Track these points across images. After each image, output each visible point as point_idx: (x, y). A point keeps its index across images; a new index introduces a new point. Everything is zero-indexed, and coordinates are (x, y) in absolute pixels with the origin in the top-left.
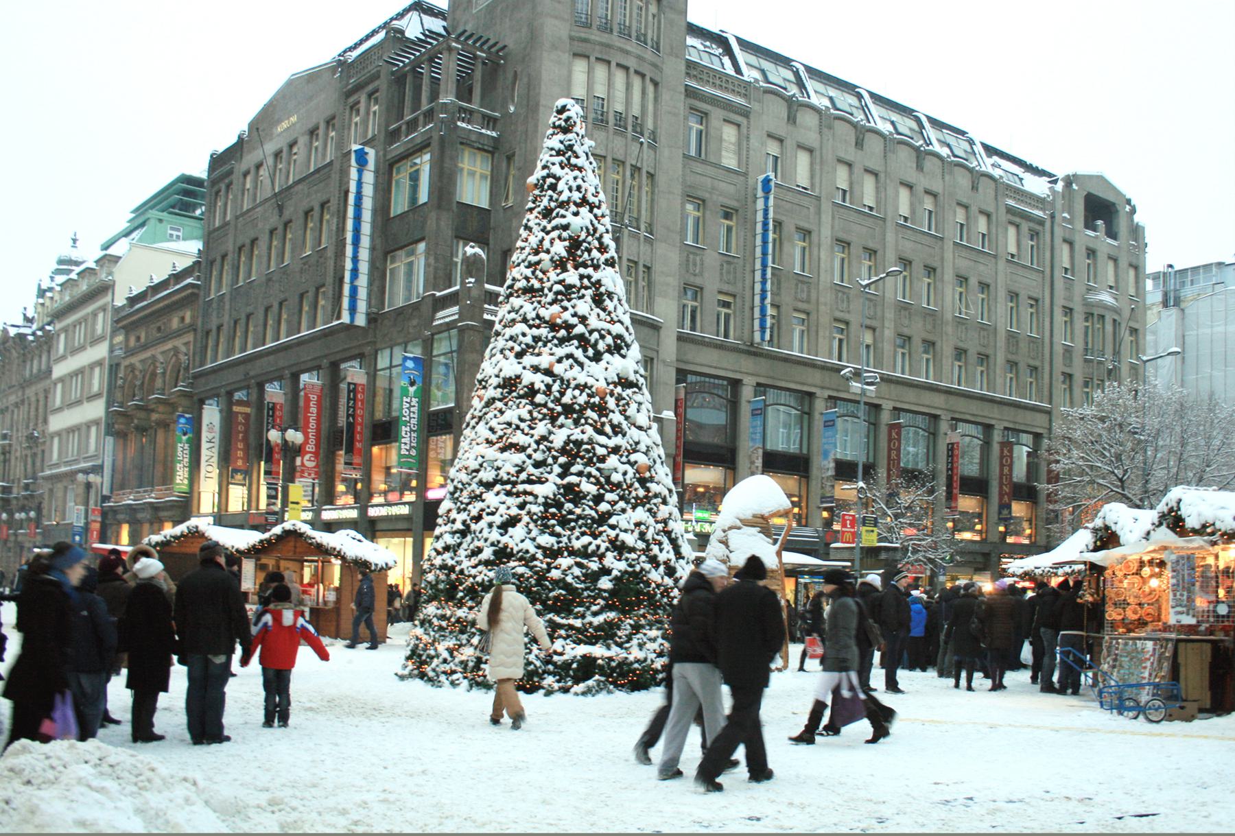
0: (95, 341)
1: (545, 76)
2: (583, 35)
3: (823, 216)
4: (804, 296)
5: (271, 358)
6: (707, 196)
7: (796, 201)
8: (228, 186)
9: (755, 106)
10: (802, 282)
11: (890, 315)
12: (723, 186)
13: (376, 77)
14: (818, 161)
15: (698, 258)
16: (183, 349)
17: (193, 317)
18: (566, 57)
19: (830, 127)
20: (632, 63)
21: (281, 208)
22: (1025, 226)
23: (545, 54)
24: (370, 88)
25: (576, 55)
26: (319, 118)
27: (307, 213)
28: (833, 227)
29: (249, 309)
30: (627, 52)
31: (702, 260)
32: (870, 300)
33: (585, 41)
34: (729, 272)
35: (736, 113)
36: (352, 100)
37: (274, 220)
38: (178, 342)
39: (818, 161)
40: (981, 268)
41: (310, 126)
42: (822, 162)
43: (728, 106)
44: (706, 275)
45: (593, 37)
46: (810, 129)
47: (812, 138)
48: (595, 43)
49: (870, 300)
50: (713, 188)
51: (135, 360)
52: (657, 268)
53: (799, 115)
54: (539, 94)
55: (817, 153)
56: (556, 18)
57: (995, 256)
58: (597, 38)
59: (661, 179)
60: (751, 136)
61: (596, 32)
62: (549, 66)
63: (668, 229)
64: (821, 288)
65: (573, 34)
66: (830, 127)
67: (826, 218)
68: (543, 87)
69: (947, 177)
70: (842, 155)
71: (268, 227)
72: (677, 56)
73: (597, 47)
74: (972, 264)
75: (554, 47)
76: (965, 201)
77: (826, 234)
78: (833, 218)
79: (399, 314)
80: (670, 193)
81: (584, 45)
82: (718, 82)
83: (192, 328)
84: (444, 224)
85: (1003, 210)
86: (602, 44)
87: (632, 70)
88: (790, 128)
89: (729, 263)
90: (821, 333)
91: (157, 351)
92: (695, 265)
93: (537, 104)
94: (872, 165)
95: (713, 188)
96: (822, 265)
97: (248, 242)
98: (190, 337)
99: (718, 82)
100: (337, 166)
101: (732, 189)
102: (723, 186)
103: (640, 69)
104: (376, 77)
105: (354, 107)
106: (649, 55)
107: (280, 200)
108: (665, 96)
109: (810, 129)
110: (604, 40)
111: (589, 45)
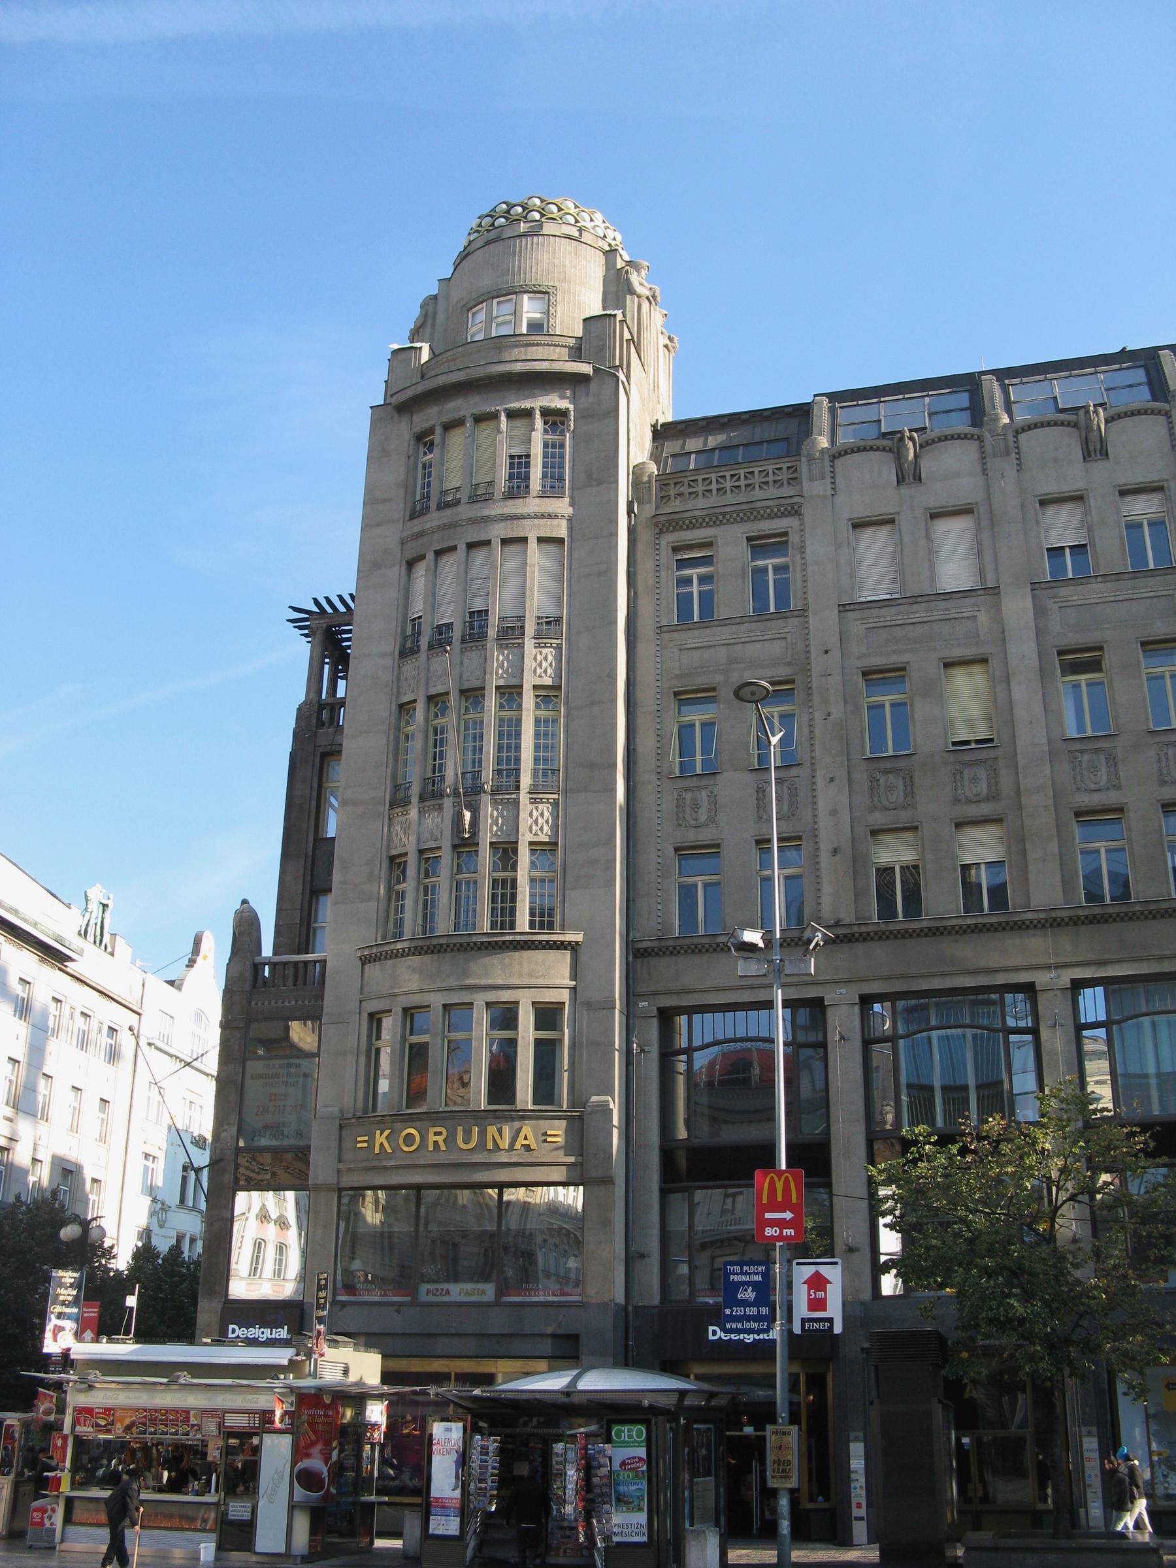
12: (753, 650)
14: (985, 522)
15: (704, 794)
35: (770, 517)
45: (429, 525)
47: (967, 489)
50: (732, 660)
60: (808, 543)
64: (1021, 761)
70: (1051, 487)
77: (1023, 651)
80: (593, 703)
90: (1033, 853)
94: (1137, 477)
96: (1020, 713)
101: (776, 648)
102: (753, 650)
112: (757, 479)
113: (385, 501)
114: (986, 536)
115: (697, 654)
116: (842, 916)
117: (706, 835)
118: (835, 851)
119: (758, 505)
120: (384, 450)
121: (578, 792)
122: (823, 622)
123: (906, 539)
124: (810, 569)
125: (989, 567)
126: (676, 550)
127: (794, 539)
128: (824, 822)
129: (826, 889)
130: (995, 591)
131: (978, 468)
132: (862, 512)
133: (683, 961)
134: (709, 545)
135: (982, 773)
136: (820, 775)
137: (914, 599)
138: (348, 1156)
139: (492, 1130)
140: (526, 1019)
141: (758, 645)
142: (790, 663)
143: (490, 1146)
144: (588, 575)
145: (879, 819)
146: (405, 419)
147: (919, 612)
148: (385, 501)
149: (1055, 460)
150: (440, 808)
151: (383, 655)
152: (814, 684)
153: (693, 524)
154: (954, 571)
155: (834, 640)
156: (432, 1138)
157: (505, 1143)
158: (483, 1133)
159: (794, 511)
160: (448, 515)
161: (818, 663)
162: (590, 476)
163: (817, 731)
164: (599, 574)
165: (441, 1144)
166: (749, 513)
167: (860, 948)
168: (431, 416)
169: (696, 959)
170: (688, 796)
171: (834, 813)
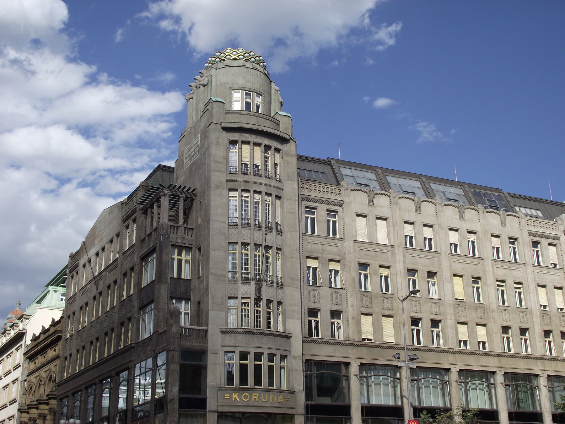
0: (15, 368)
1: (212, 204)
2: (234, 178)
3: (397, 257)
4: (389, 306)
5: (91, 372)
6: (319, 255)
7: (379, 250)
8: (77, 273)
9: (346, 200)
10: (387, 298)
11: (450, 311)
13: (134, 211)
14: (391, 224)
15: (316, 292)
16: (54, 369)
17: (59, 349)
18: (225, 192)
19: (397, 204)
20: (263, 189)
21: (97, 284)
22: (544, 242)
23: (212, 192)
24: (133, 217)
25: (230, 190)
26: (113, 234)
27: (109, 287)
28: (404, 262)
29: (83, 344)
30: (260, 184)
31: (319, 293)
32: (436, 303)
33: (236, 181)
34: (337, 298)
35: (334, 205)
36: (126, 223)
37: (94, 292)
38: (51, 366)
39: (391, 224)
40: (515, 273)
41: (110, 238)
42: (394, 225)
43: (328, 202)
44: (321, 301)
45: (239, 179)
46: (384, 207)
48: (240, 181)
49: (436, 303)
50: (323, 250)
51: (32, 378)
52: (286, 302)
53: (376, 201)
54: (210, 214)
55: (390, 220)
56: (218, 171)
57: (524, 264)
58: (242, 179)
59: (286, 250)
60: (345, 217)
61: (242, 176)
62: (216, 199)
63: (293, 279)
65: (228, 178)
66: (397, 204)
67: (399, 258)
68: (212, 210)
69: (482, 221)
71: (92, 296)
72: (292, 180)
73: (242, 184)
74: (506, 271)
75: (218, 187)
76: (497, 233)
78: (404, 256)
79: (144, 343)
80: (292, 257)
81: (235, 183)
82: (321, 189)
83: (58, 357)
84: (163, 291)
85: (526, 234)
86: (244, 182)
87: (263, 193)
88: (370, 208)
89: (337, 293)
91: (43, 373)
92: (314, 296)
93: (209, 220)
95: (323, 250)
96: (399, 286)
97: (84, 305)
98: (57, 362)
99: (321, 189)
100: (119, 261)
101: (335, 249)
102: (329, 248)
103: (269, 192)
104: (134, 211)
105: (127, 227)
106: (273, 183)
107: (96, 280)
108: (286, 203)
109: (384, 207)
110: (245, 179)
111: (237, 183)
112: (329, 190)
113: (219, 163)
114: (391, 229)
115: (313, 245)
116: (355, 338)
117: (316, 306)
118: (353, 318)
119: (332, 200)
120: (217, 142)
121: (289, 286)
122: (349, 244)
123: (371, 223)
124: (346, 226)
125: (392, 239)
126: (306, 207)
127: (340, 213)
128: (350, 309)
129: (351, 329)
130: (392, 246)
131: (389, 206)
132: (359, 212)
133: (312, 345)
134: (315, 209)
135: (390, 302)
136: (349, 293)
137: (373, 244)
138: (219, 401)
139: (271, 396)
140: (265, 358)
141: (330, 247)
142: (339, 255)
143: (271, 401)
144: (289, 213)
145: (364, 310)
146: (225, 132)
147: (374, 248)
148: (219, 163)
149: (408, 210)
150: (249, 284)
151: (222, 222)
152: (347, 264)
153: (312, 201)
154: (382, 238)
155: (352, 251)
156: (254, 397)
157: (275, 400)
158: (269, 396)
159: (341, 205)
160: (246, 178)
161: (348, 258)
162: (288, 177)
163: (348, 279)
164: (293, 213)
165: (257, 400)
166: (328, 202)
167: (360, 348)
168: (236, 136)
169: (316, 345)
170: (312, 293)
171: (352, 306)
